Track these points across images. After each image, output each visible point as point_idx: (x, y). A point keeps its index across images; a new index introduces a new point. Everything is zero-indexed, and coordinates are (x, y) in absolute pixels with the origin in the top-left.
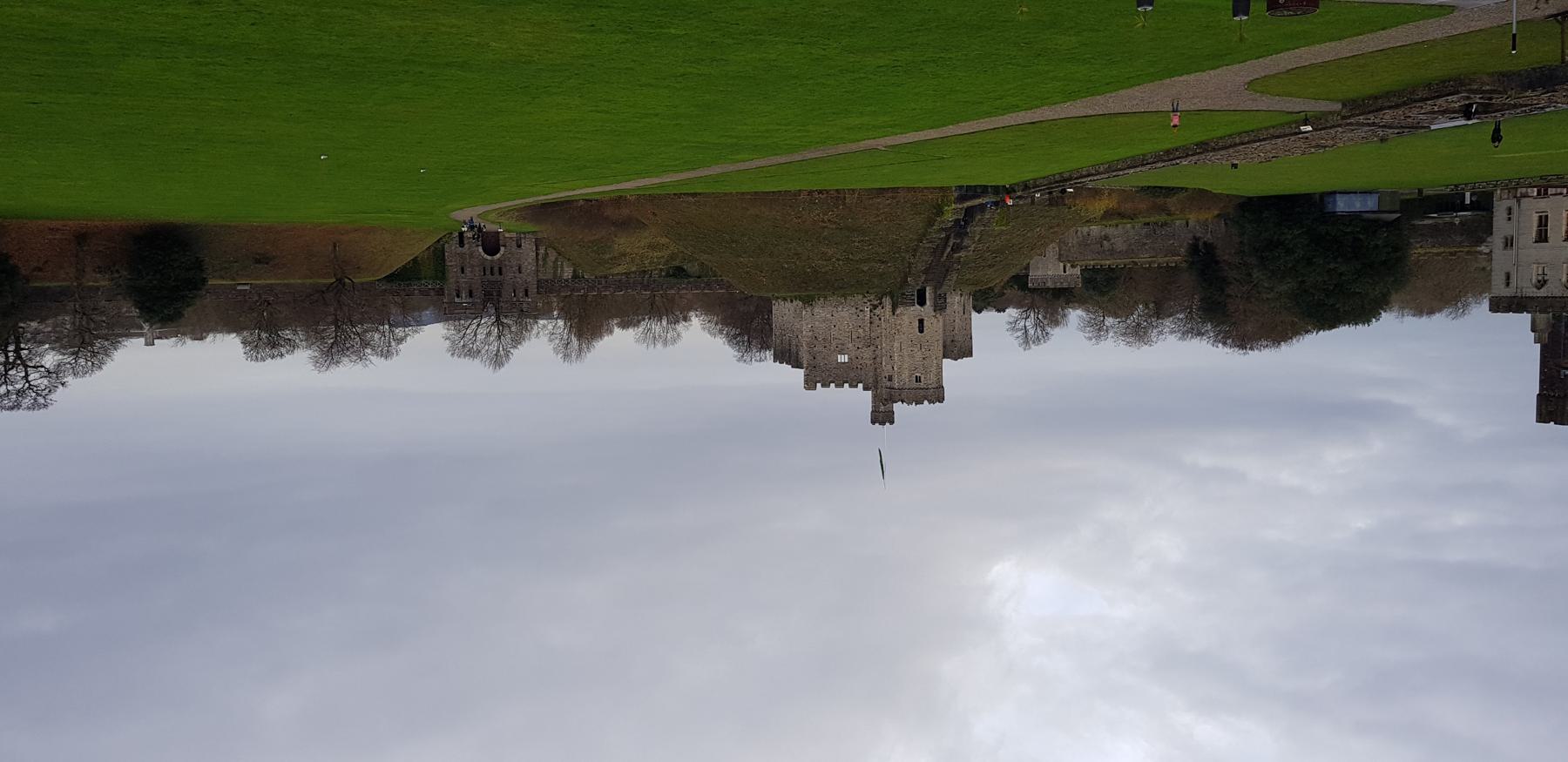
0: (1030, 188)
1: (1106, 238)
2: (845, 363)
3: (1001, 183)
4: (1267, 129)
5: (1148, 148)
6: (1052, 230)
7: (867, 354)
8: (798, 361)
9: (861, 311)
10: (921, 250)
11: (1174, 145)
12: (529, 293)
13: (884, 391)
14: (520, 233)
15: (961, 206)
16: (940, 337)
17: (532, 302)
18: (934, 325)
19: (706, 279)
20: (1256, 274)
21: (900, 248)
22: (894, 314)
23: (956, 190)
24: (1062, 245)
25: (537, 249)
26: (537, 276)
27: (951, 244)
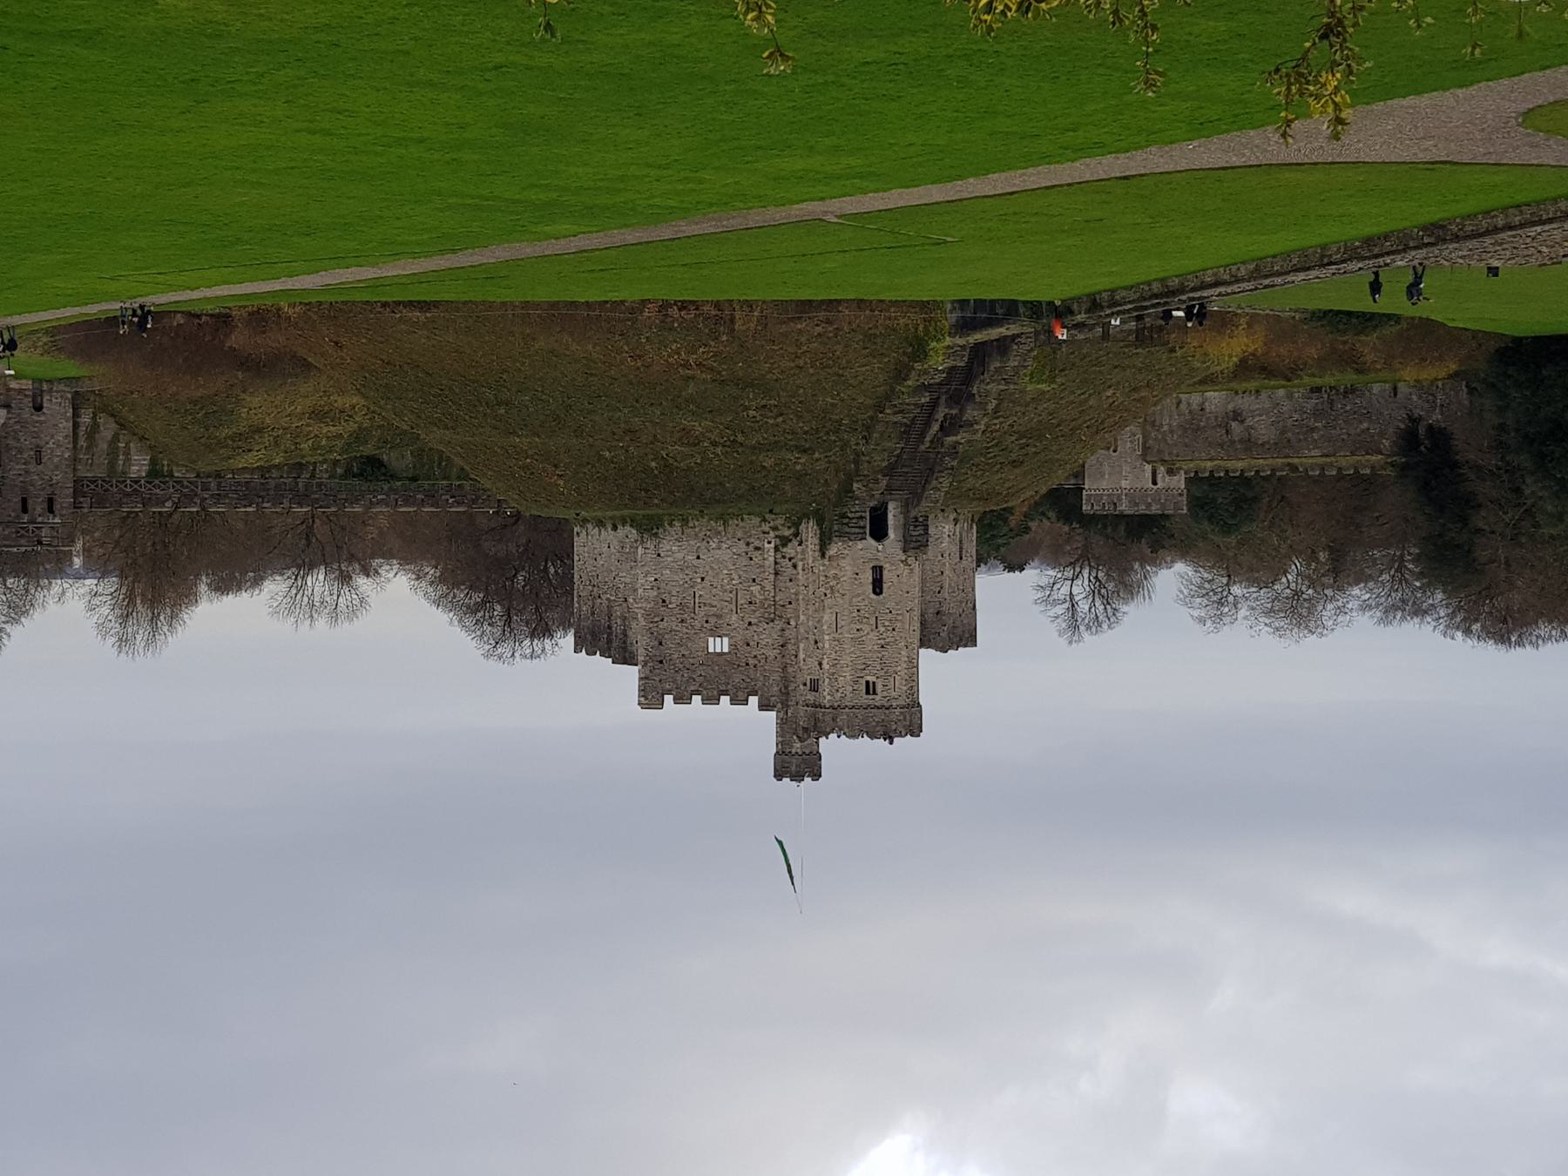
0: (1102, 308)
1: (1237, 416)
2: (722, 654)
3: (1044, 297)
4: (1555, 200)
5: (1332, 233)
6: (1136, 396)
7: (768, 636)
8: (625, 649)
9: (757, 549)
10: (880, 428)
11: (1383, 229)
12: (57, 507)
13: (802, 710)
14: (41, 381)
15: (960, 341)
16: (915, 604)
17: (63, 524)
18: (904, 578)
19: (426, 484)
20: (1531, 487)
21: (839, 422)
22: (823, 556)
23: (954, 308)
24: (1148, 428)
25: (76, 415)
26: (75, 469)
27: (940, 416)
